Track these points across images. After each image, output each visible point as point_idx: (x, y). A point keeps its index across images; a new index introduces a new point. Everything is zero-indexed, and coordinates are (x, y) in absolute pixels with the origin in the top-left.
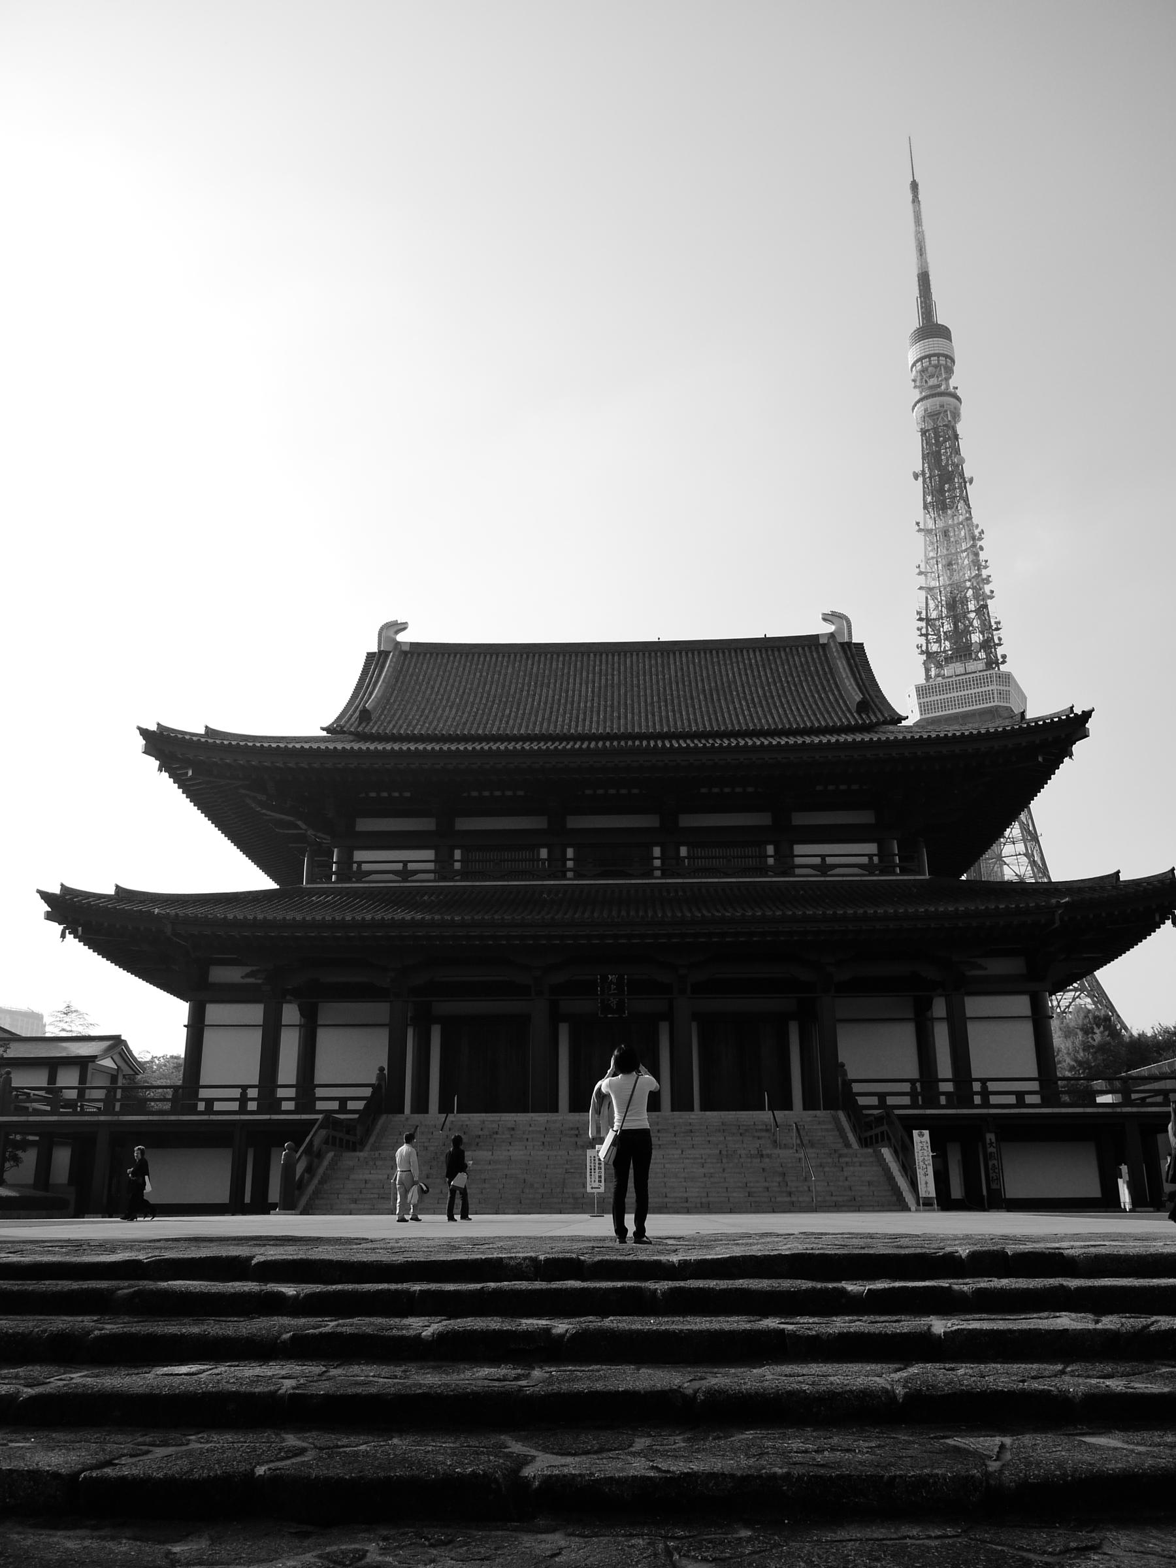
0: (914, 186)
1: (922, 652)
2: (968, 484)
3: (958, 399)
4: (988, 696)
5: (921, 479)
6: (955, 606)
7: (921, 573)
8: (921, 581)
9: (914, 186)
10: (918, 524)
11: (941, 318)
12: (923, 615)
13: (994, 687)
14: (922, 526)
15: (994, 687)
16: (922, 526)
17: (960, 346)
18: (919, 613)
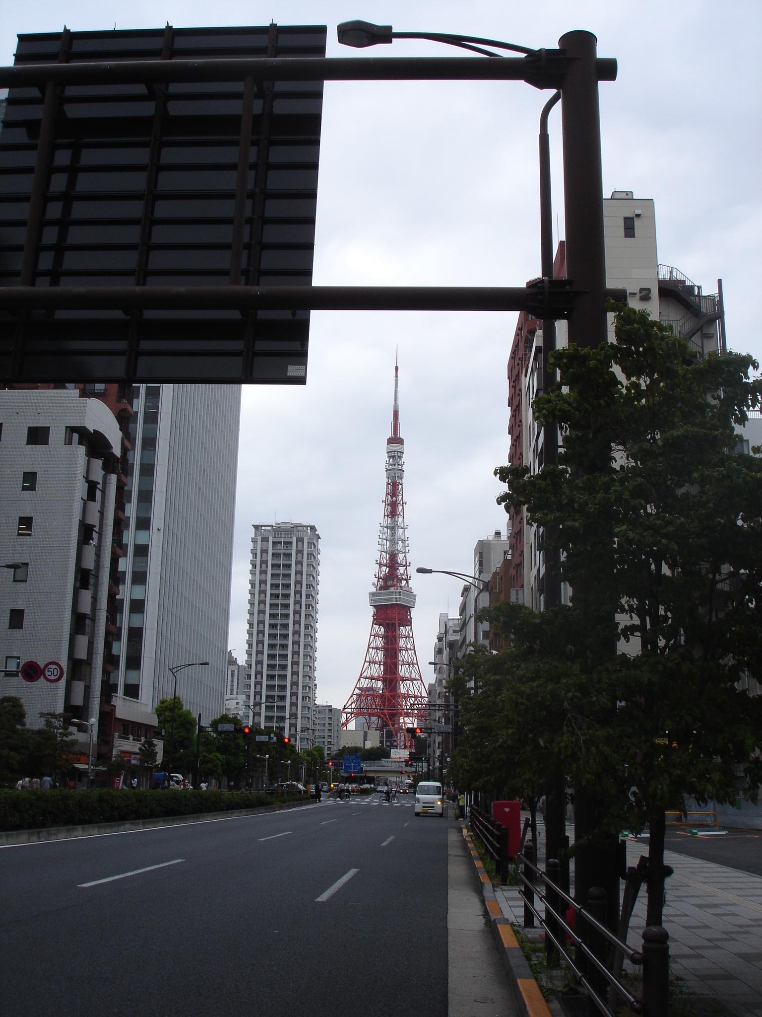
0: (397, 368)
1: (376, 577)
2: (404, 505)
3: (404, 471)
4: (392, 599)
5: (384, 503)
6: (393, 557)
7: (379, 545)
8: (379, 548)
9: (397, 368)
10: (380, 524)
11: (402, 434)
12: (378, 562)
13: (395, 596)
14: (382, 525)
15: (395, 596)
16: (382, 525)
17: (407, 447)
18: (377, 561)
